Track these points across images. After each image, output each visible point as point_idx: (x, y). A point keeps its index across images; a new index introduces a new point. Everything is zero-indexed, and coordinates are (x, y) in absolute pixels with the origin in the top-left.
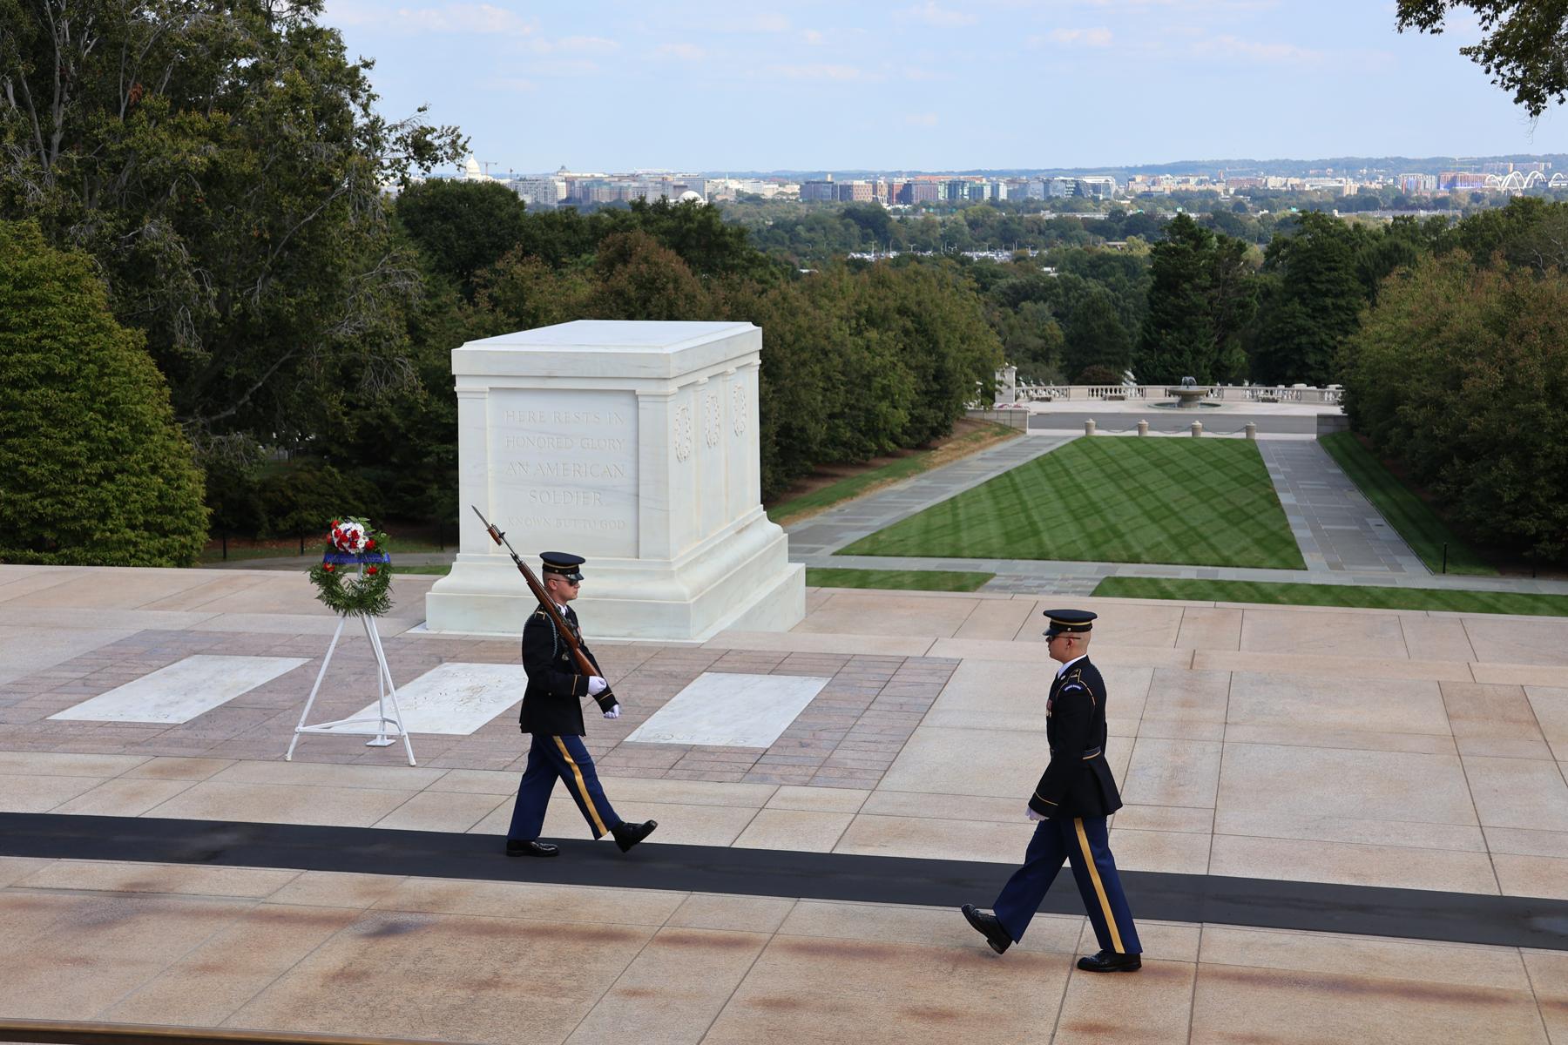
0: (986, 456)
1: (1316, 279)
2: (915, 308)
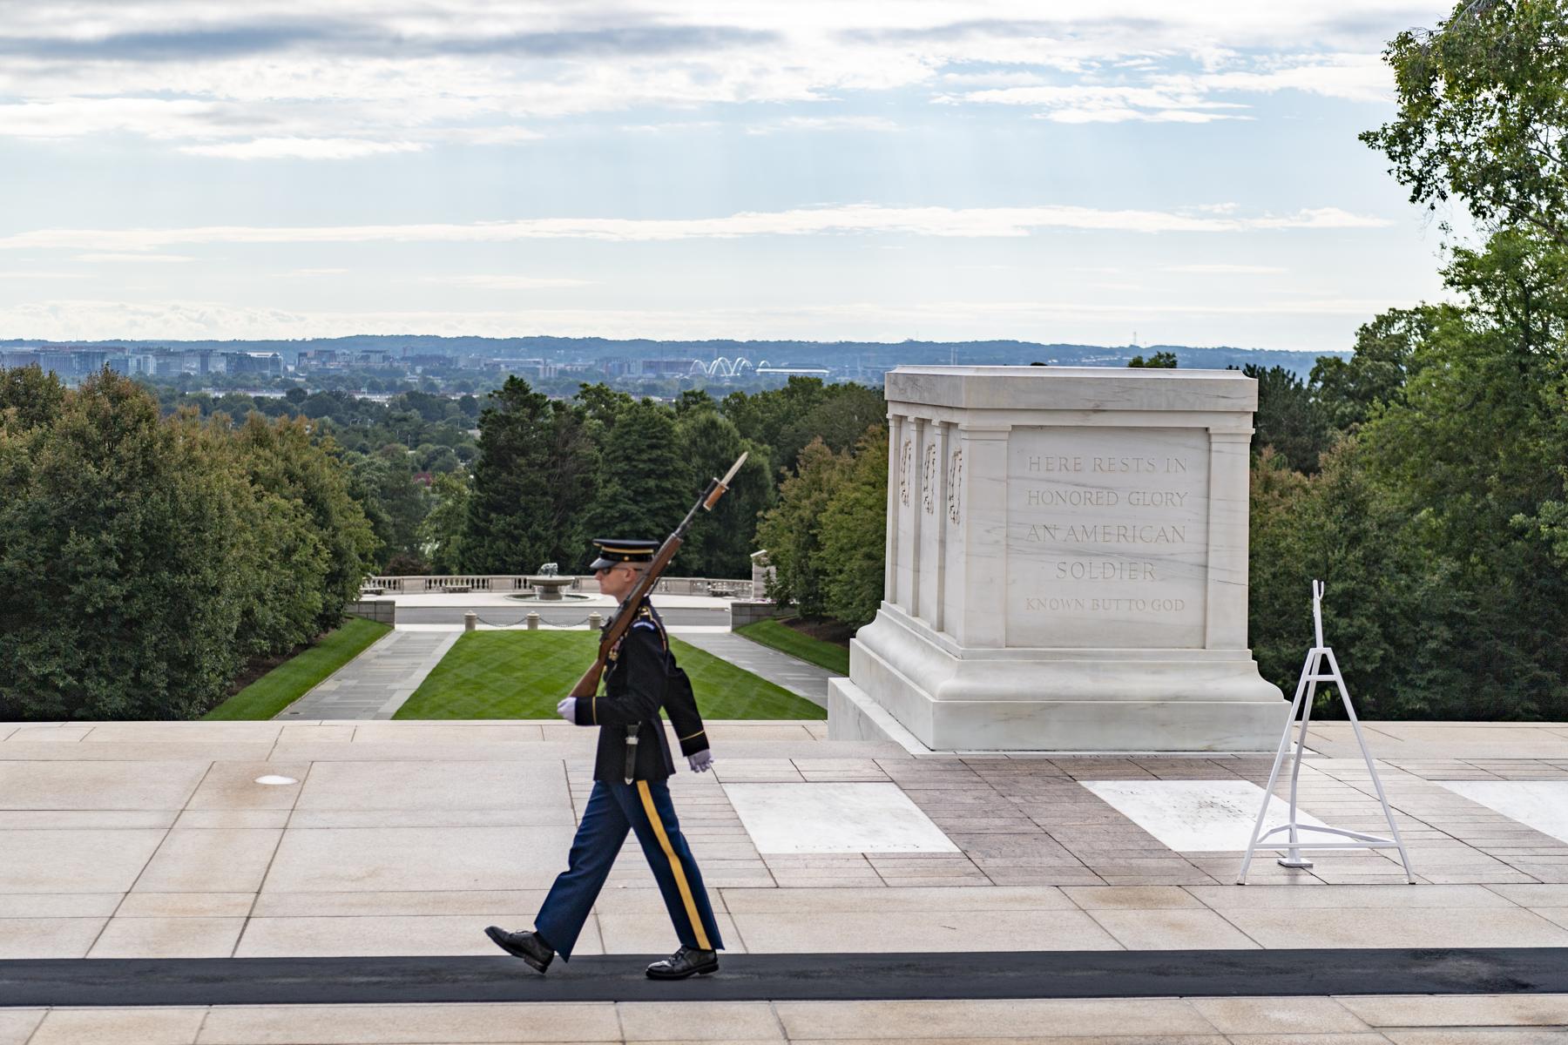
0: (381, 653)
1: (636, 458)
2: (299, 472)
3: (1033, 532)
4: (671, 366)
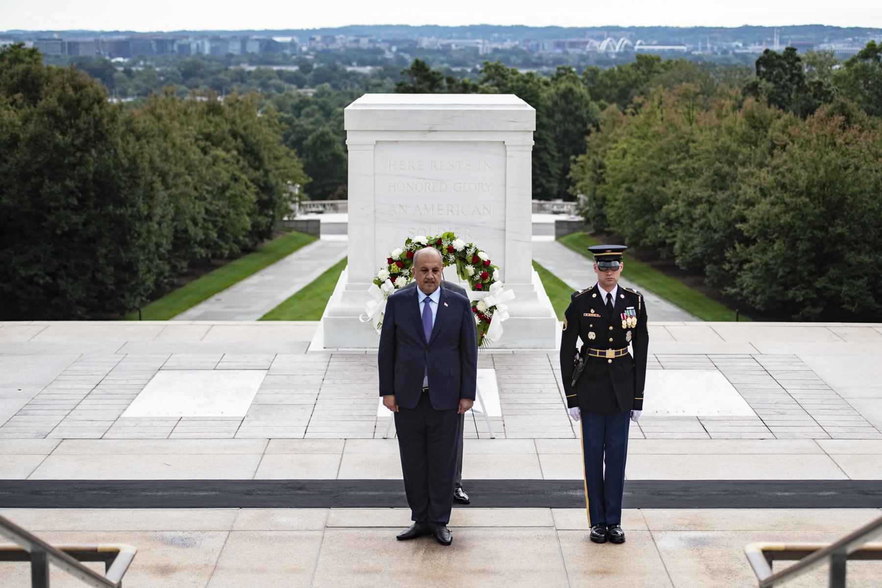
2: (242, 132)
3: (392, 209)
4: (573, 45)
